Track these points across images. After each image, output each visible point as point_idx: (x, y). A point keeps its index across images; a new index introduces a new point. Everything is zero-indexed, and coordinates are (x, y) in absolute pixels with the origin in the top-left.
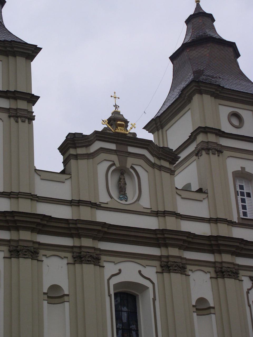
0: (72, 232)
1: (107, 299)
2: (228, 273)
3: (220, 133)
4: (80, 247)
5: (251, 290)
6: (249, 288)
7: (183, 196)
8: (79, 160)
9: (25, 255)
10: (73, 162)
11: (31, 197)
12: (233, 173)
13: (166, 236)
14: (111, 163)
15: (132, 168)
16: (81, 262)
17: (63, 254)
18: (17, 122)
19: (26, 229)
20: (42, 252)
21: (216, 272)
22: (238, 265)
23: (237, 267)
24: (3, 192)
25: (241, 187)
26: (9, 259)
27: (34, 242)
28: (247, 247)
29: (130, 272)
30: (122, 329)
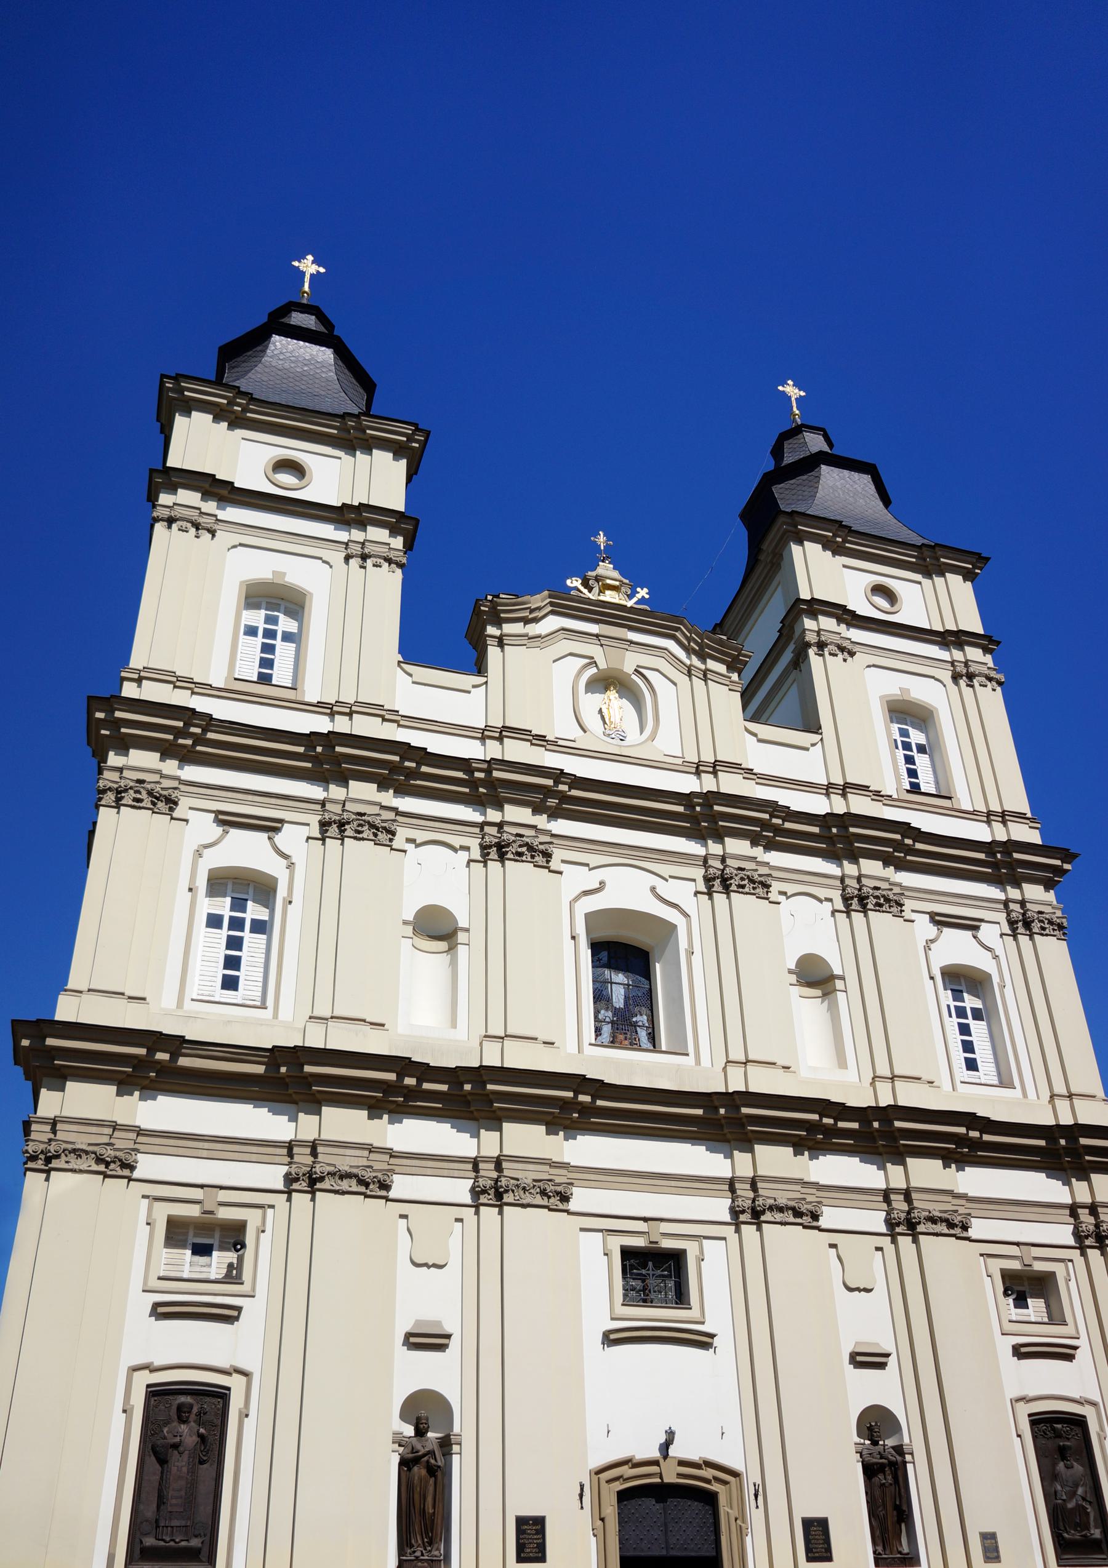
2: (875, 901)
4: (500, 826)
12: (881, 698)
17: (457, 841)
22: (900, 885)
23: (897, 890)
25: (904, 733)
29: (629, 890)
30: (612, 1022)
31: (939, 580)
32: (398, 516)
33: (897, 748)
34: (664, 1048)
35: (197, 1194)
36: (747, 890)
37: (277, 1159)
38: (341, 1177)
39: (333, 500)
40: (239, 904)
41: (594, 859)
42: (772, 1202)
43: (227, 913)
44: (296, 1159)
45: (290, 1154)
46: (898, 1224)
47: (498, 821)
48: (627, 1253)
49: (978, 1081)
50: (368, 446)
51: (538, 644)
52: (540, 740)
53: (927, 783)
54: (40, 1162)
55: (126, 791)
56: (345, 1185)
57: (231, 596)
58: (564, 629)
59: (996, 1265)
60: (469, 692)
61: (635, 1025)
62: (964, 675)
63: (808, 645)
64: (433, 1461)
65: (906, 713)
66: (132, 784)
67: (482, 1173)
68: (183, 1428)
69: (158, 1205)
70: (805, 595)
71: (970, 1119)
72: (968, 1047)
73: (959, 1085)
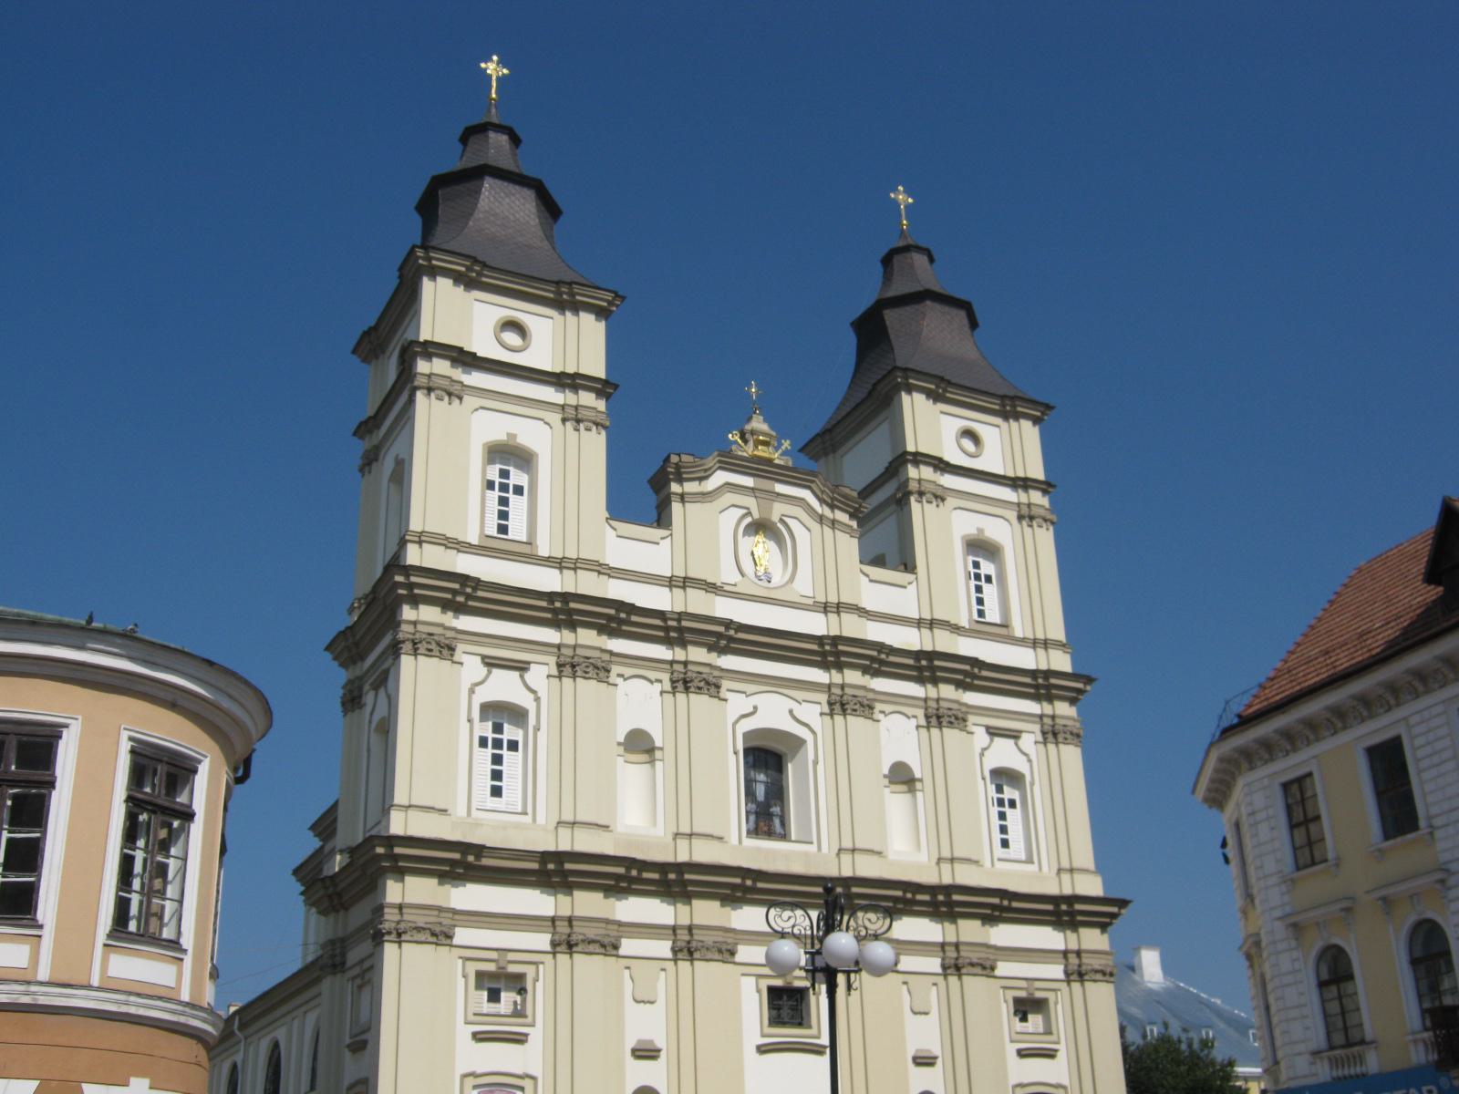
1: (732, 758)
2: (948, 719)
3: (941, 465)
4: (685, 663)
5: (990, 750)
6: (985, 745)
7: (872, 577)
9: (586, 672)
14: (745, 511)
15: (782, 521)
17: (652, 675)
23: (964, 709)
24: (549, 557)
25: (976, 565)
27: (603, 651)
29: (774, 713)
33: (970, 578)
35: (494, 955)
36: (858, 713)
38: (589, 943)
40: (498, 728)
41: (750, 688)
43: (490, 736)
44: (558, 929)
45: (554, 926)
46: (949, 968)
48: (771, 990)
50: (576, 307)
52: (712, 588)
53: (993, 615)
54: (393, 936)
55: (420, 642)
56: (591, 948)
57: (477, 455)
59: (1011, 994)
60: (658, 544)
62: (1026, 516)
63: (910, 493)
65: (980, 547)
66: (424, 636)
67: (679, 937)
69: (468, 963)
70: (911, 448)
72: (1003, 830)
73: (995, 860)
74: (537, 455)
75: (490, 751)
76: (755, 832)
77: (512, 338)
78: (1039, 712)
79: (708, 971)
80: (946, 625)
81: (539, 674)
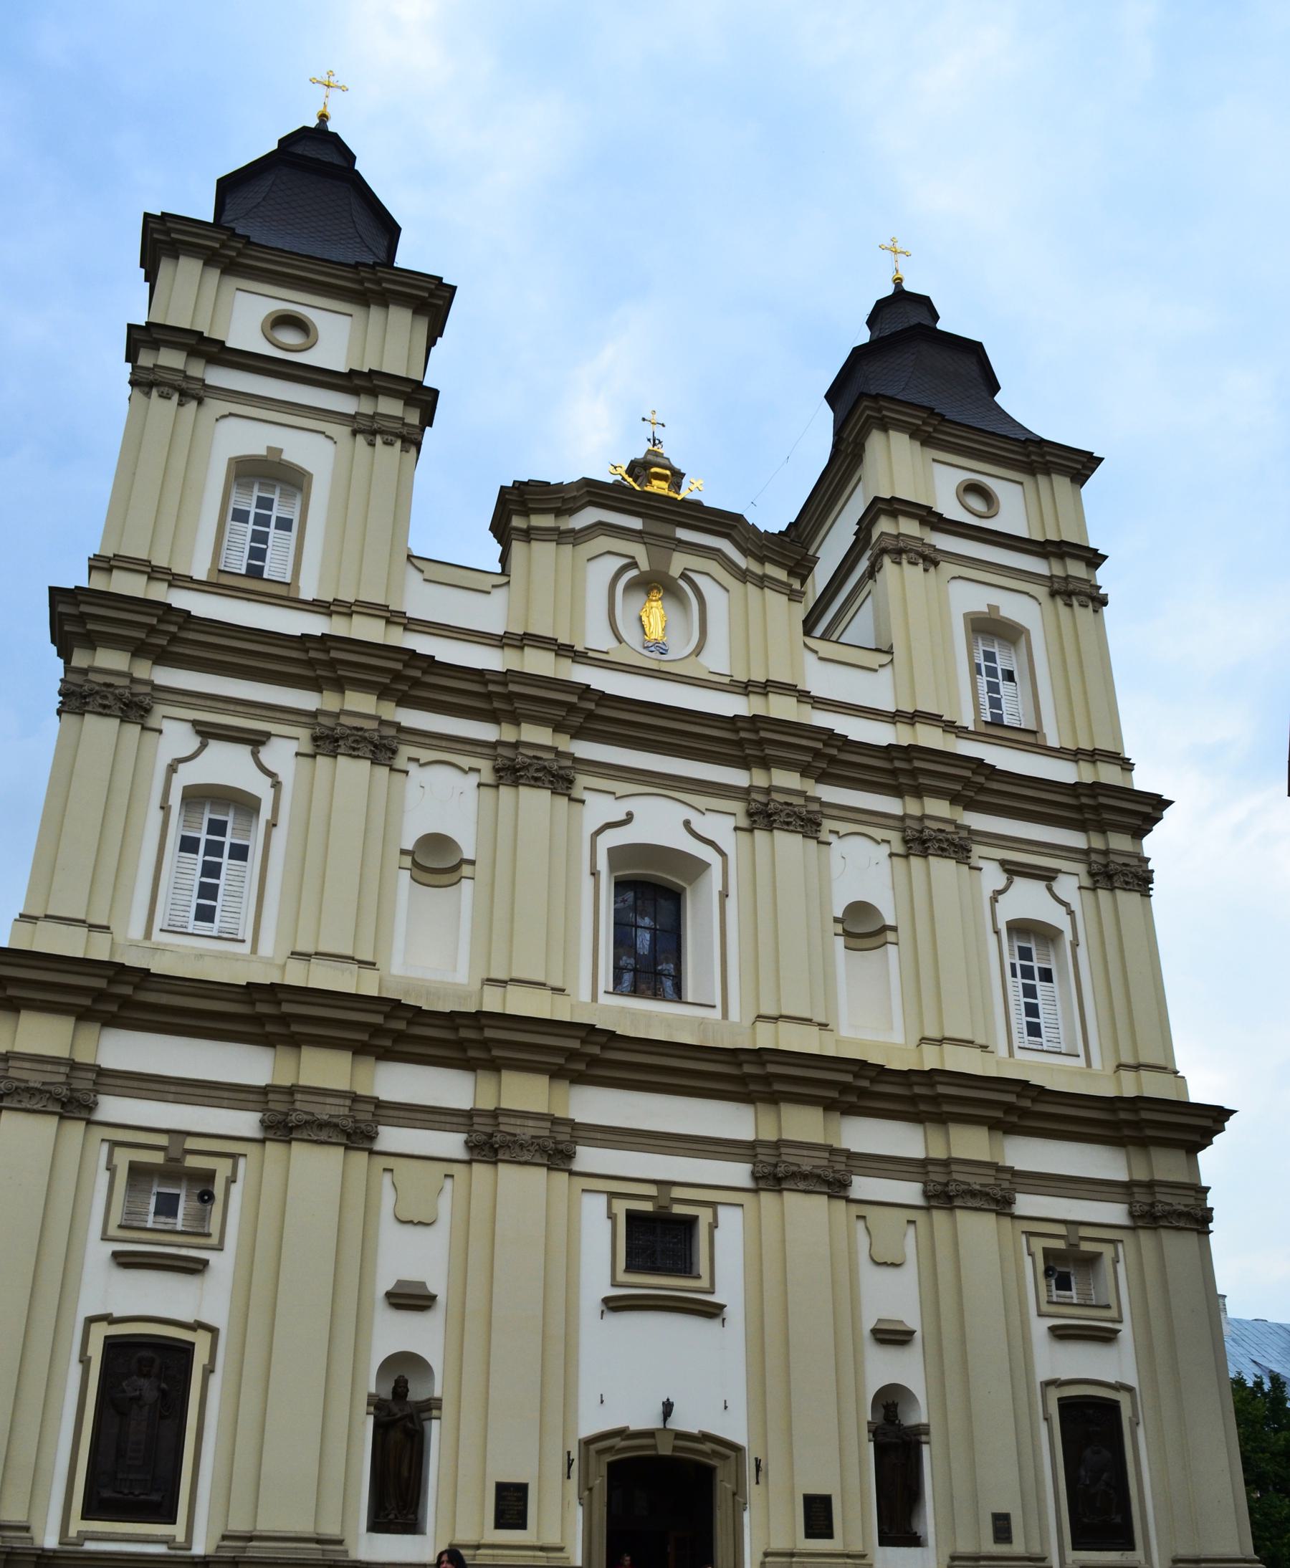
0: (496, 705)
1: (588, 882)
4: (516, 745)
6: (1000, 887)
7: (821, 655)
8: (534, 544)
9: (354, 749)
10: (517, 547)
11: (388, 615)
13: (763, 734)
16: (515, 784)
18: (372, 444)
19: (363, 686)
20: (406, 751)
21: (905, 841)
22: (968, 828)
23: (964, 834)
26: (309, 760)
27: (383, 723)
28: (995, 786)
29: (659, 823)
30: (635, 970)
31: (1042, 479)
32: (413, 386)
34: (690, 1000)
37: (251, 1105)
39: (339, 364)
40: (217, 827)
42: (795, 1169)
43: (203, 836)
47: (513, 740)
49: (1039, 1047)
51: (571, 540)
58: (600, 524)
61: (658, 975)
64: (410, 1425)
68: (144, 1383)
71: (1023, 1087)
72: (1032, 1010)
74: (311, 475)
75: (200, 857)
76: (618, 988)
77: (289, 337)
78: (1084, 845)
79: (521, 1184)
80: (933, 719)
81: (282, 753)
